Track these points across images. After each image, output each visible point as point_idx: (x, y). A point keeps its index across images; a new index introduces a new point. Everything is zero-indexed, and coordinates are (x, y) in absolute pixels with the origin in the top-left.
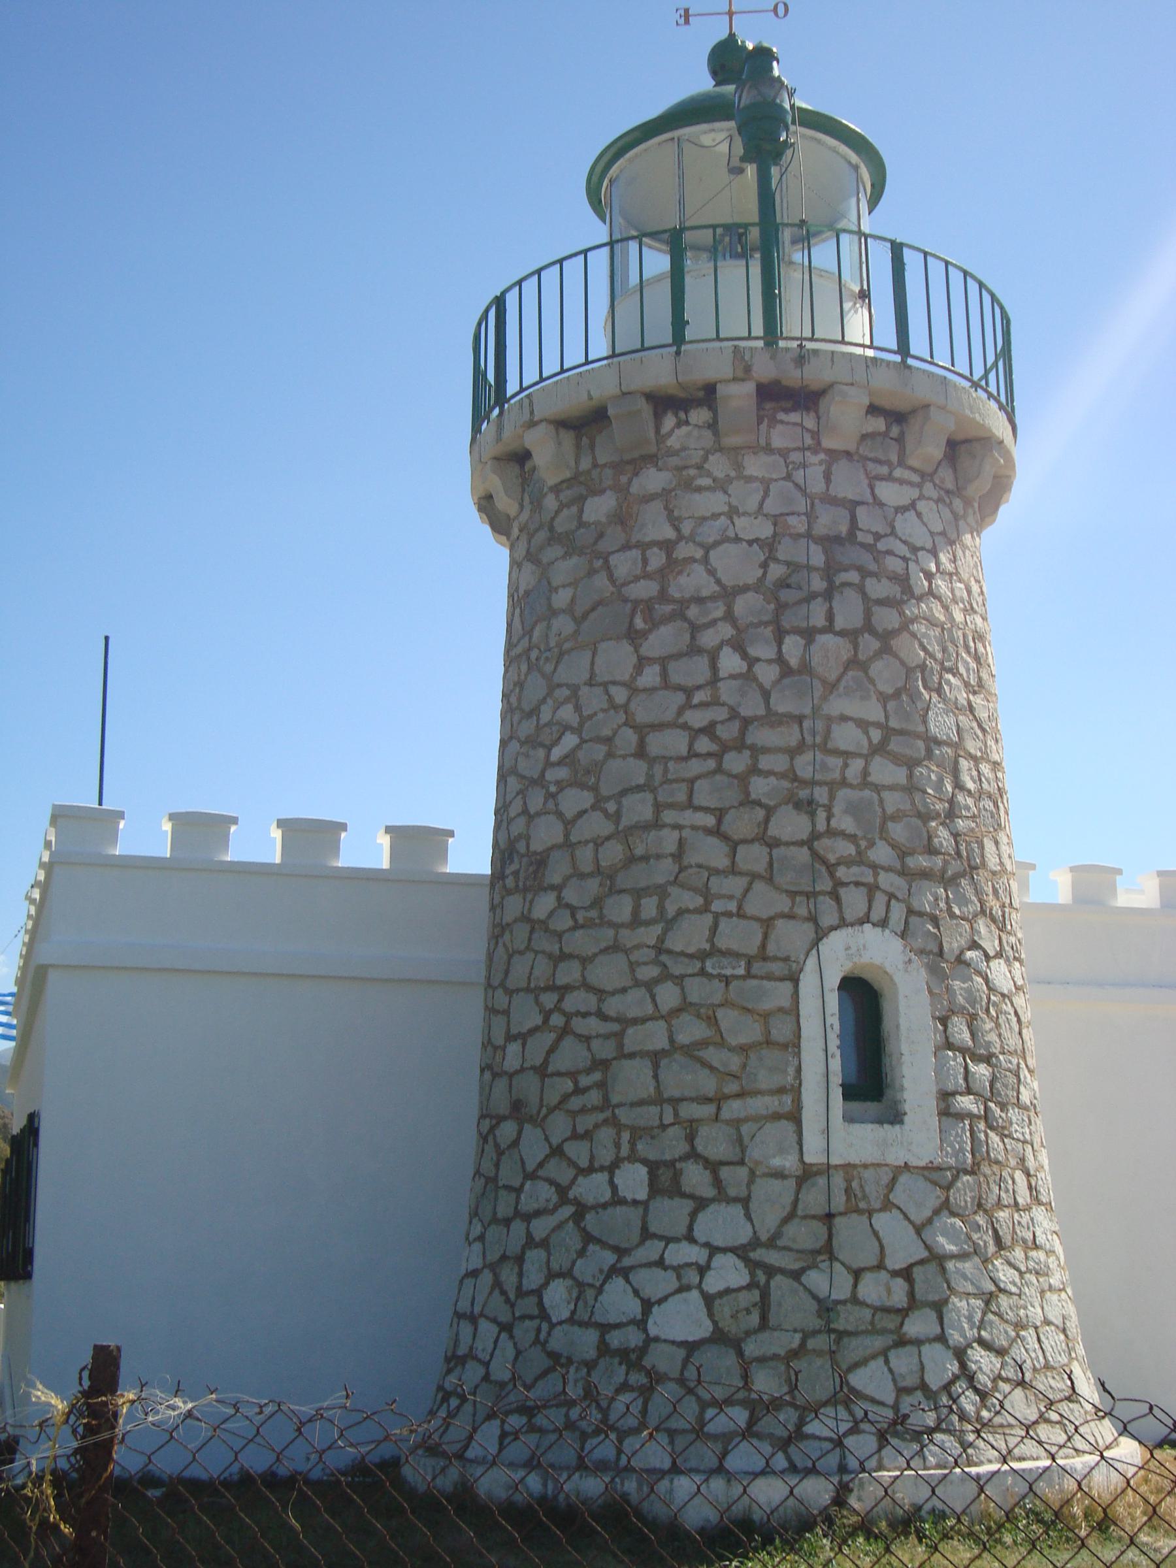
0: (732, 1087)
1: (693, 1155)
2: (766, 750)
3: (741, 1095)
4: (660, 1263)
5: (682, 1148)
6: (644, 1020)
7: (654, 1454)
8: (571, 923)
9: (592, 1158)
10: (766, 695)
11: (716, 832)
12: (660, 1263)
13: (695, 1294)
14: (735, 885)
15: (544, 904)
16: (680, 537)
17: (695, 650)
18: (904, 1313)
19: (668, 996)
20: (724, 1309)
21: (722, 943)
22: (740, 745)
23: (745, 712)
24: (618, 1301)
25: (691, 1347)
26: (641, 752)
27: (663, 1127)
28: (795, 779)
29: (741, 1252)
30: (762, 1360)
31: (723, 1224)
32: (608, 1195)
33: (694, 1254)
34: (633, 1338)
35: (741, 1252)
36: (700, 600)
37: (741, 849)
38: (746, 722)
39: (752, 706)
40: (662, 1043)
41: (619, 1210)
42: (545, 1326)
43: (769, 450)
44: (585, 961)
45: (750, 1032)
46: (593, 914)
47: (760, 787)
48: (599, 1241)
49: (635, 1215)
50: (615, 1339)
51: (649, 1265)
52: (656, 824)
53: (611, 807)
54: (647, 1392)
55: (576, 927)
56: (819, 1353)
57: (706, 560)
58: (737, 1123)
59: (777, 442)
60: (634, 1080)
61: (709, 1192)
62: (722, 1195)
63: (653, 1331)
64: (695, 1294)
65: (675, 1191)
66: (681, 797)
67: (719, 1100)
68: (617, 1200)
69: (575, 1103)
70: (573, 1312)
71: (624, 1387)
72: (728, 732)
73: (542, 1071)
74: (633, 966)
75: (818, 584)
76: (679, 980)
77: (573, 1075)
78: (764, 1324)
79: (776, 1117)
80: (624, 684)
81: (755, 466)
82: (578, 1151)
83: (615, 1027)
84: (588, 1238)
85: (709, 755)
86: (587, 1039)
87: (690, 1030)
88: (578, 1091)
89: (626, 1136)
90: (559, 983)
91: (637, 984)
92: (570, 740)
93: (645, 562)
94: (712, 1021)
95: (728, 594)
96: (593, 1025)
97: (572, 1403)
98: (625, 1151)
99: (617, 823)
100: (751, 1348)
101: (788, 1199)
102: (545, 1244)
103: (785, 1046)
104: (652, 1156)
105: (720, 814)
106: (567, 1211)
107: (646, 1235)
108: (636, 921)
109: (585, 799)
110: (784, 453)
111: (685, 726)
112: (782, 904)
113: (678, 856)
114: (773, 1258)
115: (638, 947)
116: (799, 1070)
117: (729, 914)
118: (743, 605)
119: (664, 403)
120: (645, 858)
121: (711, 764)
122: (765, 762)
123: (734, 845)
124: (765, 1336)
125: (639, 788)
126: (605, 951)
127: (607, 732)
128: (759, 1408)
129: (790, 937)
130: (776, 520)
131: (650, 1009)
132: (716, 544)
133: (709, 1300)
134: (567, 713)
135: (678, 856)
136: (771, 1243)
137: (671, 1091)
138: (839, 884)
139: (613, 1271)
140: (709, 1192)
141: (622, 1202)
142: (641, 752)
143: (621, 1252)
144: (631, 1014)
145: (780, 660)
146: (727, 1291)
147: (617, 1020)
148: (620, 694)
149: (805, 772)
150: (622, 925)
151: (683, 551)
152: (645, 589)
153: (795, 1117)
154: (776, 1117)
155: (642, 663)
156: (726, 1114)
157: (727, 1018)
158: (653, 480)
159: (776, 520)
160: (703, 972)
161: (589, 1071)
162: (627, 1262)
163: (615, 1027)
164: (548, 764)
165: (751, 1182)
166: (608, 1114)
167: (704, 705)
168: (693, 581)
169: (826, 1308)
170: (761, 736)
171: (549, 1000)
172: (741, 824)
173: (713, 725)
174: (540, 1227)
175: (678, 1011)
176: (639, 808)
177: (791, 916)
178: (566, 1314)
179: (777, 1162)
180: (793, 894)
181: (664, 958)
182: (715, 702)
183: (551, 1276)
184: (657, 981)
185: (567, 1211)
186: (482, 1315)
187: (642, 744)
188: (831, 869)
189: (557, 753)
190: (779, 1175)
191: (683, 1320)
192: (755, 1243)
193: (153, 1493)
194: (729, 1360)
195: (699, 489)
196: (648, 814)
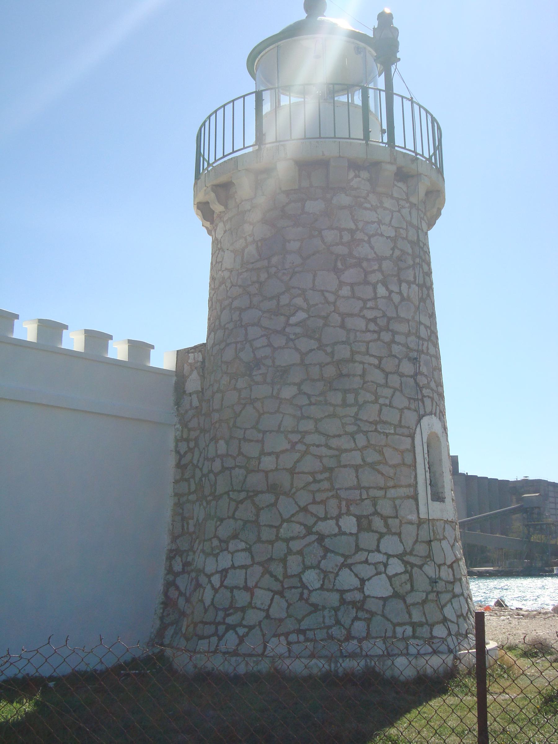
0: (391, 483)
1: (376, 513)
2: (397, 333)
3: (394, 487)
4: (366, 562)
5: (371, 510)
6: (351, 450)
7: (377, 648)
8: (307, 402)
9: (326, 513)
10: (396, 308)
11: (379, 367)
12: (366, 562)
13: (383, 576)
14: (388, 392)
15: (288, 392)
16: (357, 229)
17: (366, 282)
18: (453, 583)
19: (361, 440)
20: (397, 582)
21: (384, 418)
22: (387, 329)
23: (389, 315)
24: (347, 579)
25: (385, 599)
26: (343, 326)
27: (362, 500)
28: (408, 347)
29: (400, 557)
30: (414, 604)
31: (390, 545)
32: (336, 530)
33: (380, 558)
34: (358, 596)
35: (400, 557)
36: (368, 260)
37: (390, 376)
38: (390, 319)
39: (391, 313)
40: (359, 461)
41: (344, 537)
42: (306, 591)
43: (392, 197)
44: (317, 421)
45: (395, 459)
46: (321, 398)
47: (396, 349)
48: (332, 552)
49: (352, 539)
50: (348, 597)
51: (361, 563)
52: (352, 360)
53: (329, 349)
54: (368, 621)
55: (311, 404)
56: (432, 601)
57: (369, 242)
58: (393, 499)
59: (395, 195)
60: (346, 478)
61: (384, 530)
62: (390, 532)
63: (367, 593)
64: (383, 576)
65: (369, 529)
66: (363, 349)
67: (385, 489)
68: (342, 533)
69: (314, 487)
70: (322, 585)
71: (356, 618)
72: (382, 322)
73: (292, 472)
74: (344, 425)
75: (410, 262)
76: (366, 433)
77: (312, 474)
78: (412, 589)
79: (408, 497)
80: (332, 293)
81: (388, 203)
82: (319, 510)
83: (336, 453)
84: (327, 550)
85: (375, 332)
86: (320, 457)
87: (372, 457)
88: (315, 481)
89: (344, 503)
90: (300, 429)
91: (346, 433)
92: (301, 315)
93: (341, 237)
94: (381, 453)
95: (380, 259)
96: (324, 451)
97: (330, 627)
98: (344, 510)
99: (333, 357)
100: (409, 600)
101: (414, 534)
102: (300, 553)
103: (409, 466)
104: (357, 513)
105: (380, 359)
106: (313, 537)
107: (358, 549)
108: (344, 404)
109: (314, 344)
110: (398, 200)
111: (364, 317)
112: (406, 403)
113: (363, 376)
114: (412, 559)
115: (346, 416)
116: (416, 477)
117: (386, 405)
118: (386, 265)
119: (355, 166)
120: (348, 375)
121: (375, 336)
122: (398, 338)
123: (387, 374)
124: (413, 594)
125: (343, 343)
126: (329, 416)
127: (323, 314)
128: (414, 625)
129: (410, 417)
130: (396, 229)
131: (353, 445)
132: (373, 236)
133: (390, 578)
134: (299, 301)
135: (363, 376)
136: (411, 553)
137: (365, 484)
138: (423, 396)
139: (343, 565)
140: (384, 530)
141: (344, 534)
142: (343, 326)
143: (346, 557)
144: (343, 447)
145: (400, 293)
146: (396, 575)
147: (337, 450)
148: (331, 298)
149: (412, 346)
150: (337, 405)
151: (359, 235)
152: (341, 250)
153: (415, 498)
154: (408, 497)
155: (341, 284)
156: (389, 495)
157: (388, 452)
158: (344, 199)
159: (396, 229)
160: (376, 430)
161: (321, 472)
162: (349, 561)
163: (336, 453)
164: (287, 324)
165: (400, 526)
166: (334, 493)
167: (371, 308)
168: (363, 250)
169: (434, 582)
170: (396, 326)
171: (295, 438)
172: (389, 365)
173: (376, 318)
174: (296, 546)
175: (366, 447)
176: (344, 352)
177: (409, 409)
178: (318, 585)
179: (410, 517)
180: (409, 399)
181: (358, 422)
182: (376, 308)
183: (306, 568)
184: (356, 432)
185: (313, 537)
186: (256, 586)
187: (343, 321)
188: (421, 389)
189: (293, 320)
190: (411, 523)
191: (378, 587)
192: (405, 553)
193: (51, 684)
194: (400, 605)
195: (366, 209)
196: (348, 355)
